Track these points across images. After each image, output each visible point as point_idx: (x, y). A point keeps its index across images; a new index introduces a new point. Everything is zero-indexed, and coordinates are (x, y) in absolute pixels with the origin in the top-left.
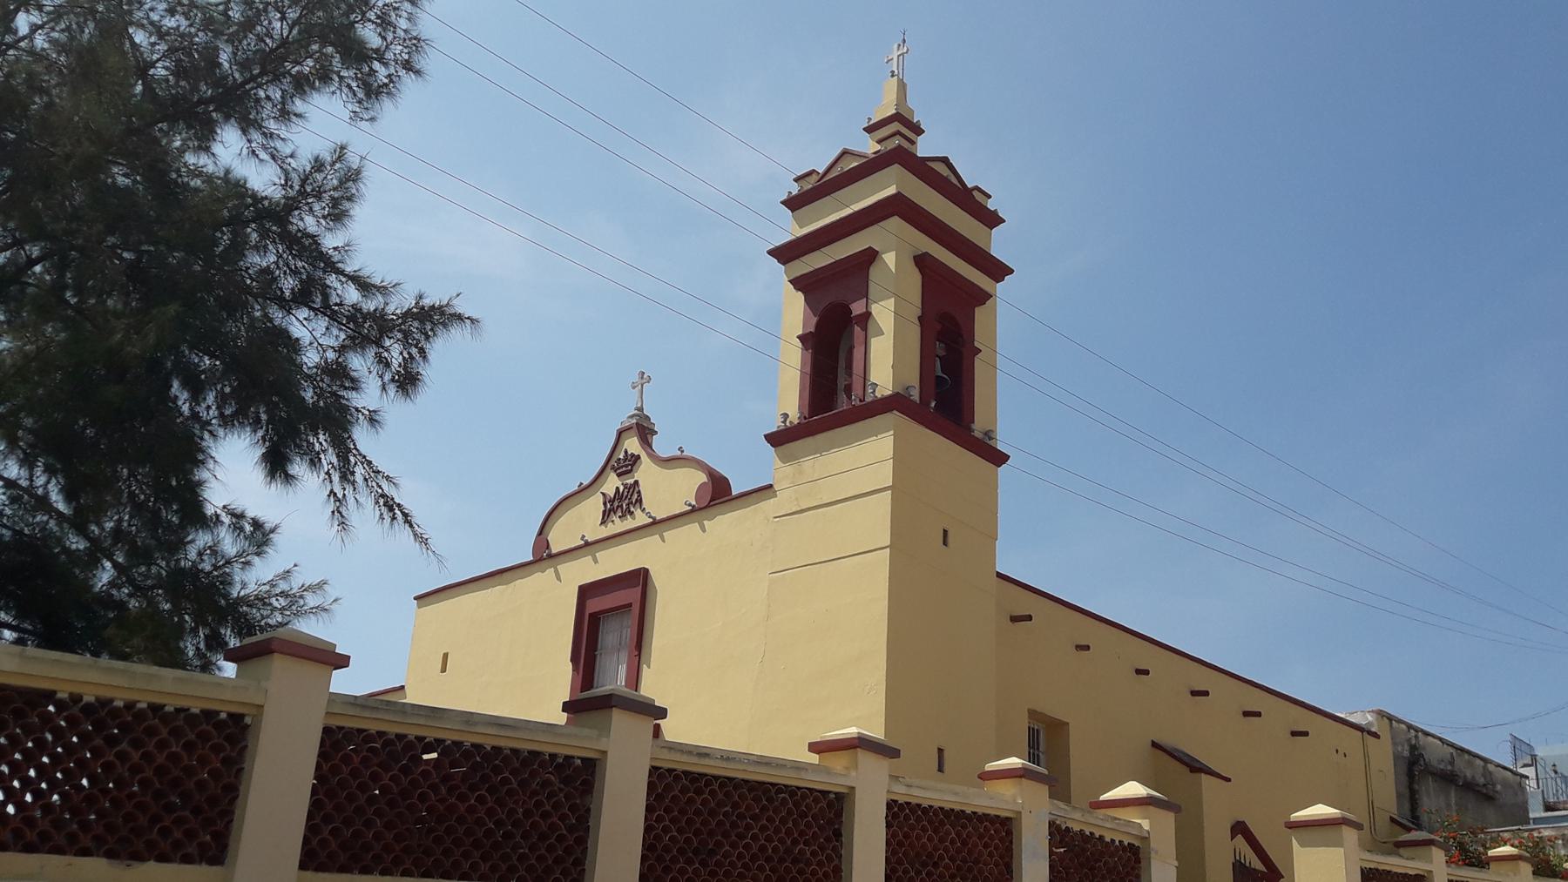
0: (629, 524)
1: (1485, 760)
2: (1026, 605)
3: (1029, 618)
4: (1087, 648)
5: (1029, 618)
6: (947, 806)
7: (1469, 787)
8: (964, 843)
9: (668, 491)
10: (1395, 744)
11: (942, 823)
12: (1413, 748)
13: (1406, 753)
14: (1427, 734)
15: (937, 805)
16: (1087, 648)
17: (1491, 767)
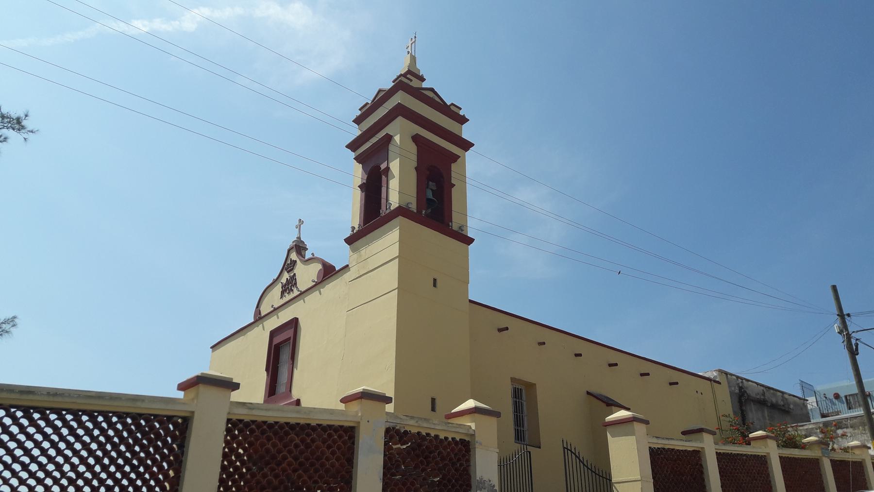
0: (292, 295)
1: (783, 393)
2: (505, 322)
3: (507, 329)
4: (544, 343)
5: (507, 329)
6: (293, 422)
7: (774, 407)
8: (308, 446)
9: (306, 275)
10: (730, 387)
11: (287, 434)
12: (741, 388)
13: (737, 391)
14: (748, 380)
15: (282, 421)
16: (544, 343)
17: (786, 396)
